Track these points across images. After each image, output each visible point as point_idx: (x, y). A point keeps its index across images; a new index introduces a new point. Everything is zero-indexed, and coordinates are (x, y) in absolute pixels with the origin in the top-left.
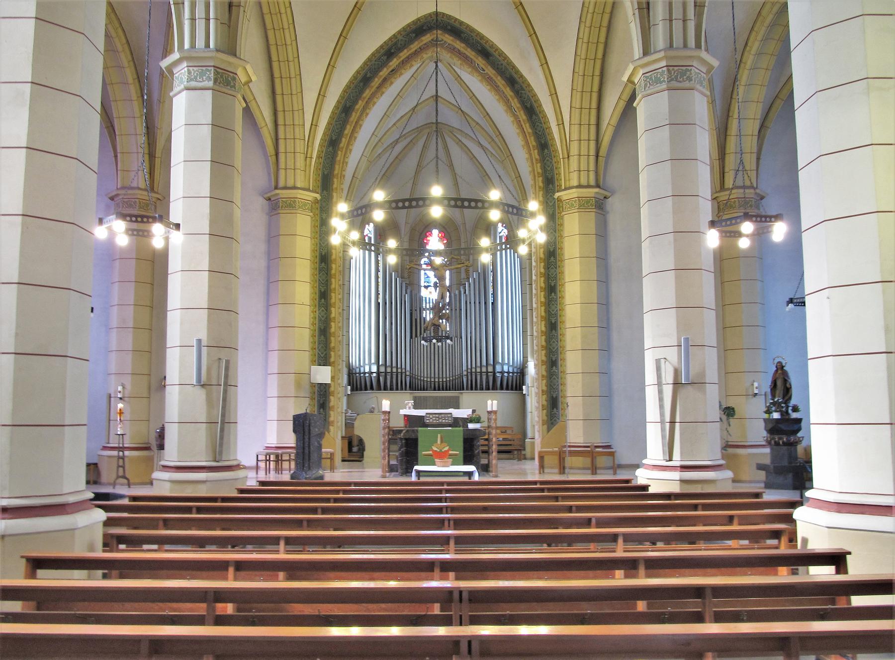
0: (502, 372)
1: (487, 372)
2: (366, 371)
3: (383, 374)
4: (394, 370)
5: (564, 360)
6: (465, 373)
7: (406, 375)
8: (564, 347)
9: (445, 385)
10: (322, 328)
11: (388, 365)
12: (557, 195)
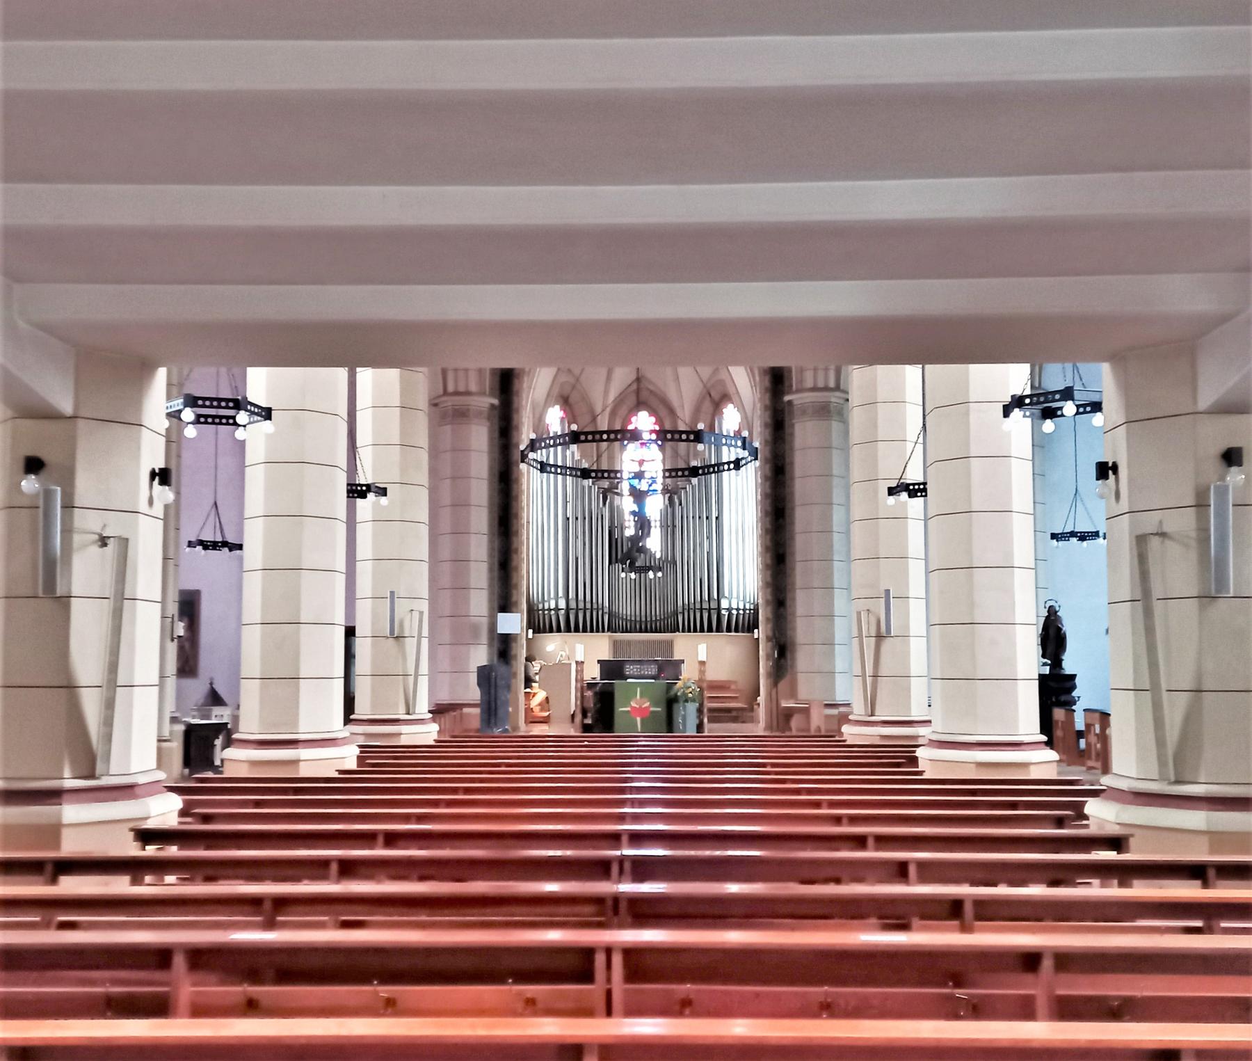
0: (729, 610)
1: (710, 609)
2: (552, 608)
4: (588, 606)
5: (794, 599)
6: (680, 610)
8: (794, 584)
12: (787, 398)
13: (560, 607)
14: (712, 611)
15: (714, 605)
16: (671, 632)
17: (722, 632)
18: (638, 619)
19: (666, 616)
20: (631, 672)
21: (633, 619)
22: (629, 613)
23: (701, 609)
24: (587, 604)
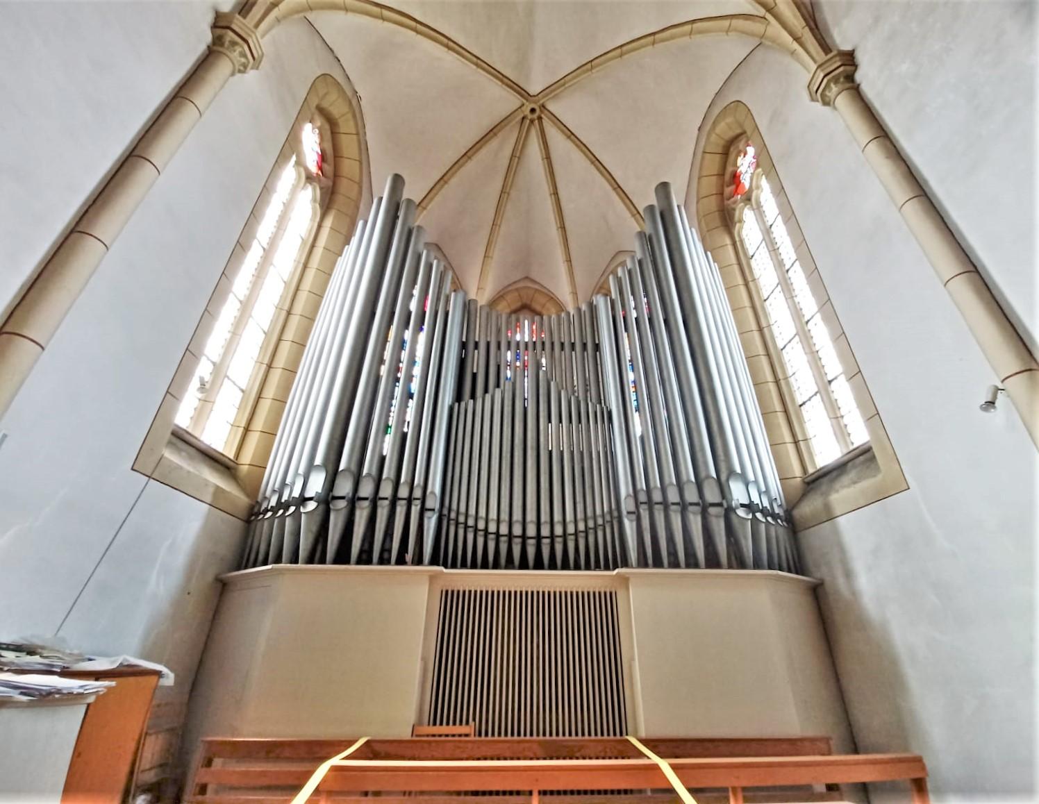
4: (386, 490)
6: (627, 505)
7: (423, 510)
9: (559, 548)
13: (307, 495)
14: (712, 510)
15: (712, 495)
18: (517, 530)
19: (591, 524)
21: (504, 530)
22: (493, 515)
24: (383, 485)
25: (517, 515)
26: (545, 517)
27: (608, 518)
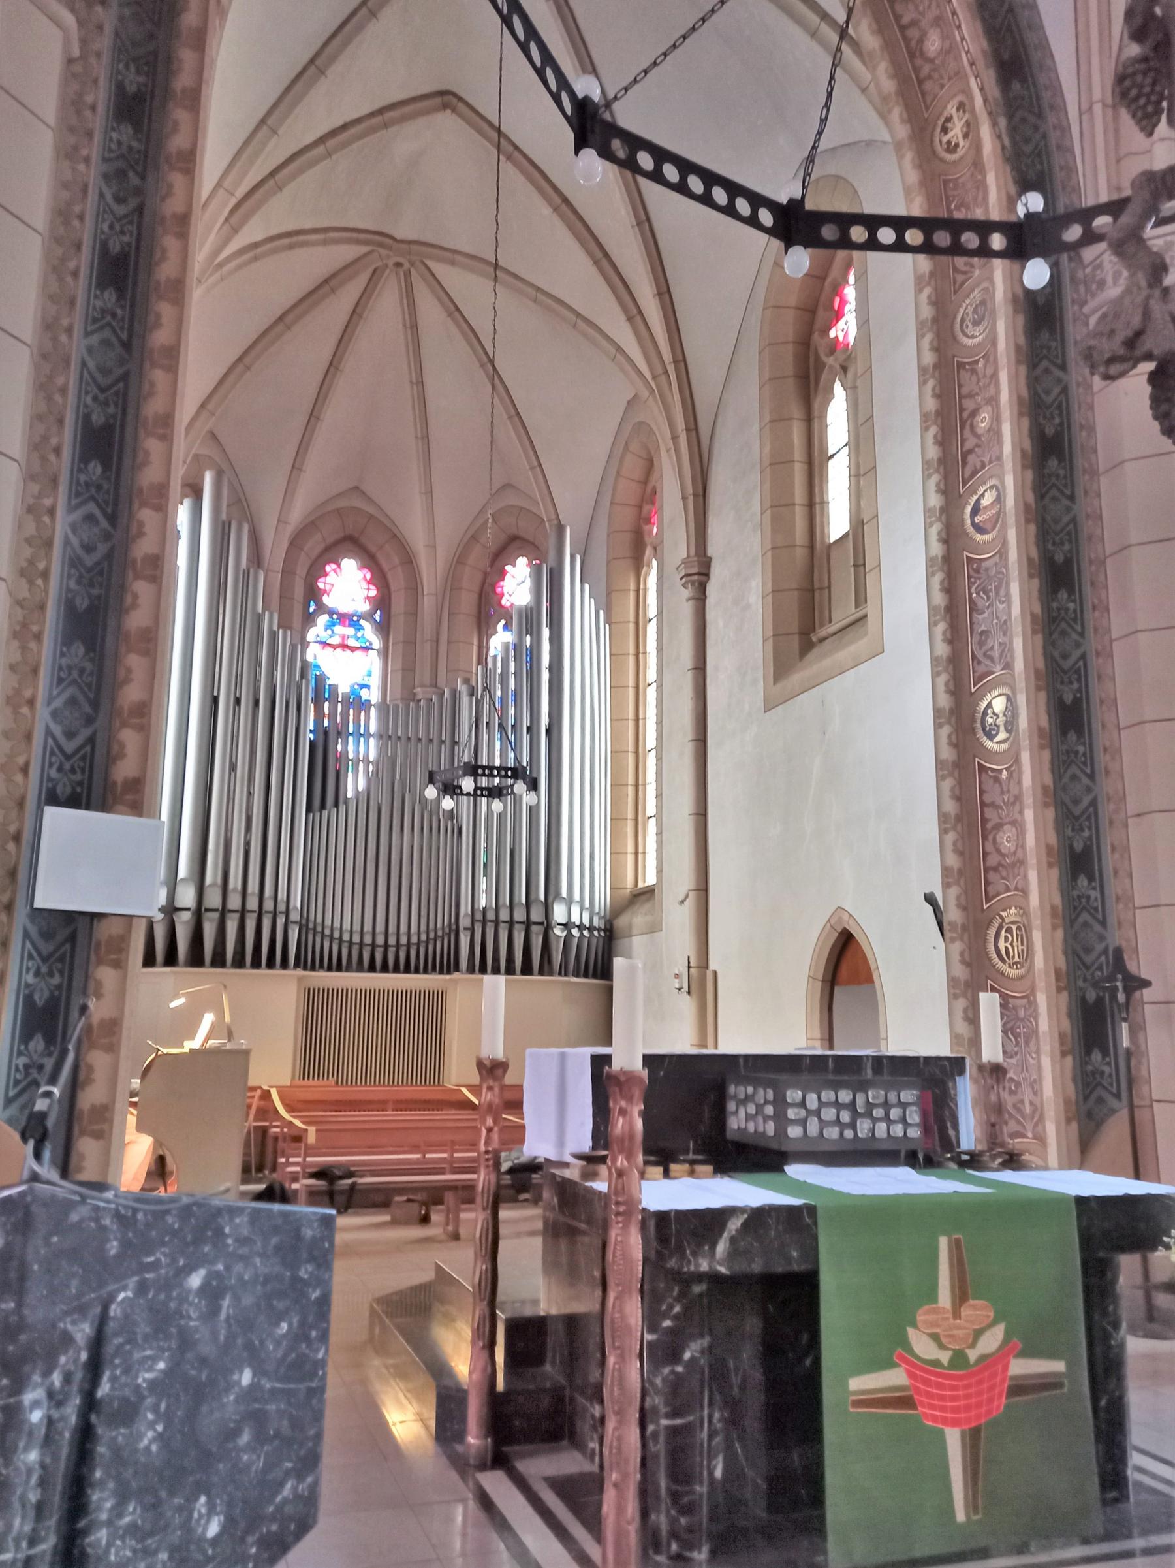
3: (216, 915)
4: (252, 904)
10: (82, 604)
11: (231, 885)
13: (178, 905)
14: (534, 928)
15: (537, 915)
16: (441, 972)
17: (551, 974)
18: (368, 939)
19: (432, 935)
20: (813, 1127)
21: (356, 939)
22: (347, 926)
23: (511, 923)
25: (368, 927)
26: (392, 928)
27: (447, 930)
